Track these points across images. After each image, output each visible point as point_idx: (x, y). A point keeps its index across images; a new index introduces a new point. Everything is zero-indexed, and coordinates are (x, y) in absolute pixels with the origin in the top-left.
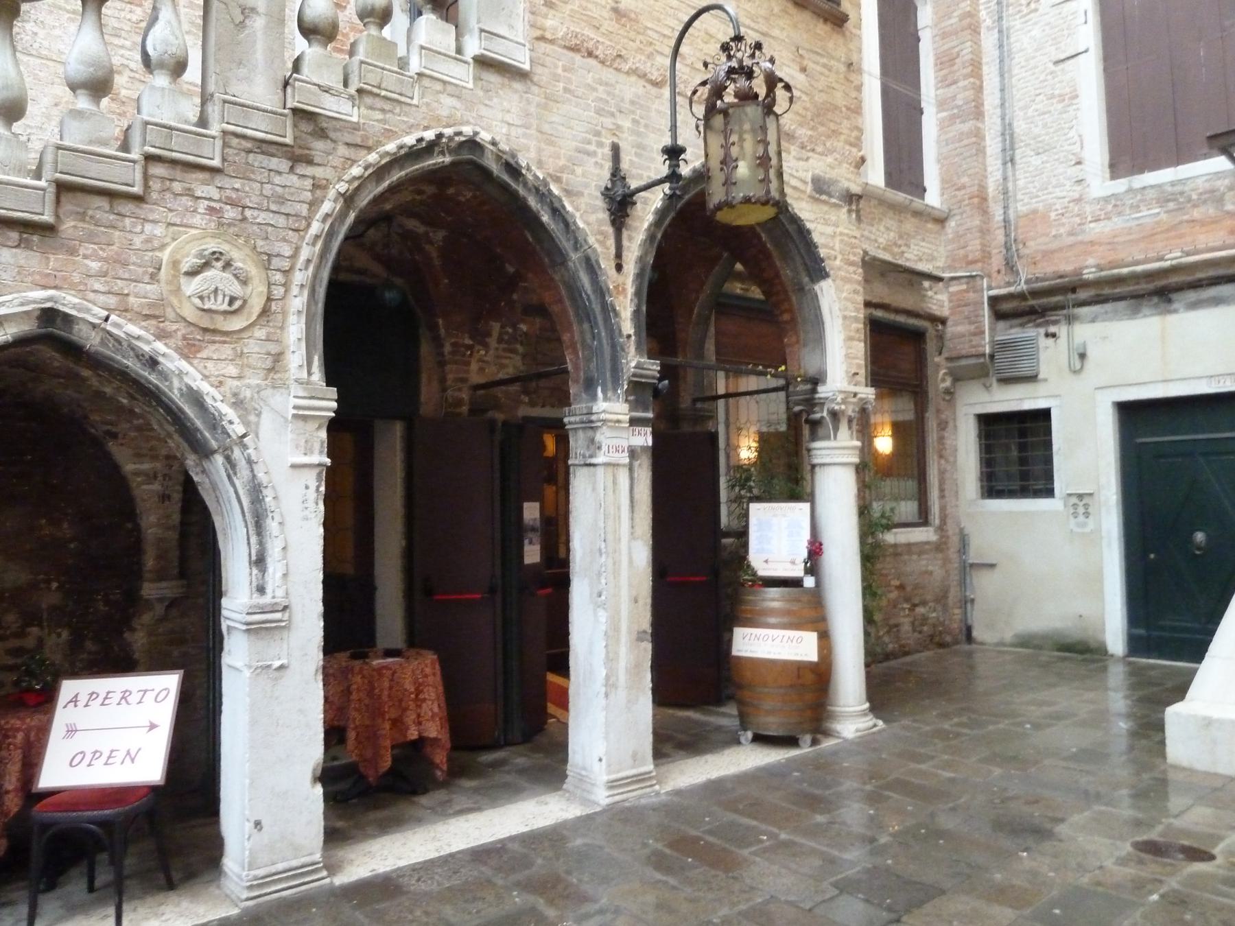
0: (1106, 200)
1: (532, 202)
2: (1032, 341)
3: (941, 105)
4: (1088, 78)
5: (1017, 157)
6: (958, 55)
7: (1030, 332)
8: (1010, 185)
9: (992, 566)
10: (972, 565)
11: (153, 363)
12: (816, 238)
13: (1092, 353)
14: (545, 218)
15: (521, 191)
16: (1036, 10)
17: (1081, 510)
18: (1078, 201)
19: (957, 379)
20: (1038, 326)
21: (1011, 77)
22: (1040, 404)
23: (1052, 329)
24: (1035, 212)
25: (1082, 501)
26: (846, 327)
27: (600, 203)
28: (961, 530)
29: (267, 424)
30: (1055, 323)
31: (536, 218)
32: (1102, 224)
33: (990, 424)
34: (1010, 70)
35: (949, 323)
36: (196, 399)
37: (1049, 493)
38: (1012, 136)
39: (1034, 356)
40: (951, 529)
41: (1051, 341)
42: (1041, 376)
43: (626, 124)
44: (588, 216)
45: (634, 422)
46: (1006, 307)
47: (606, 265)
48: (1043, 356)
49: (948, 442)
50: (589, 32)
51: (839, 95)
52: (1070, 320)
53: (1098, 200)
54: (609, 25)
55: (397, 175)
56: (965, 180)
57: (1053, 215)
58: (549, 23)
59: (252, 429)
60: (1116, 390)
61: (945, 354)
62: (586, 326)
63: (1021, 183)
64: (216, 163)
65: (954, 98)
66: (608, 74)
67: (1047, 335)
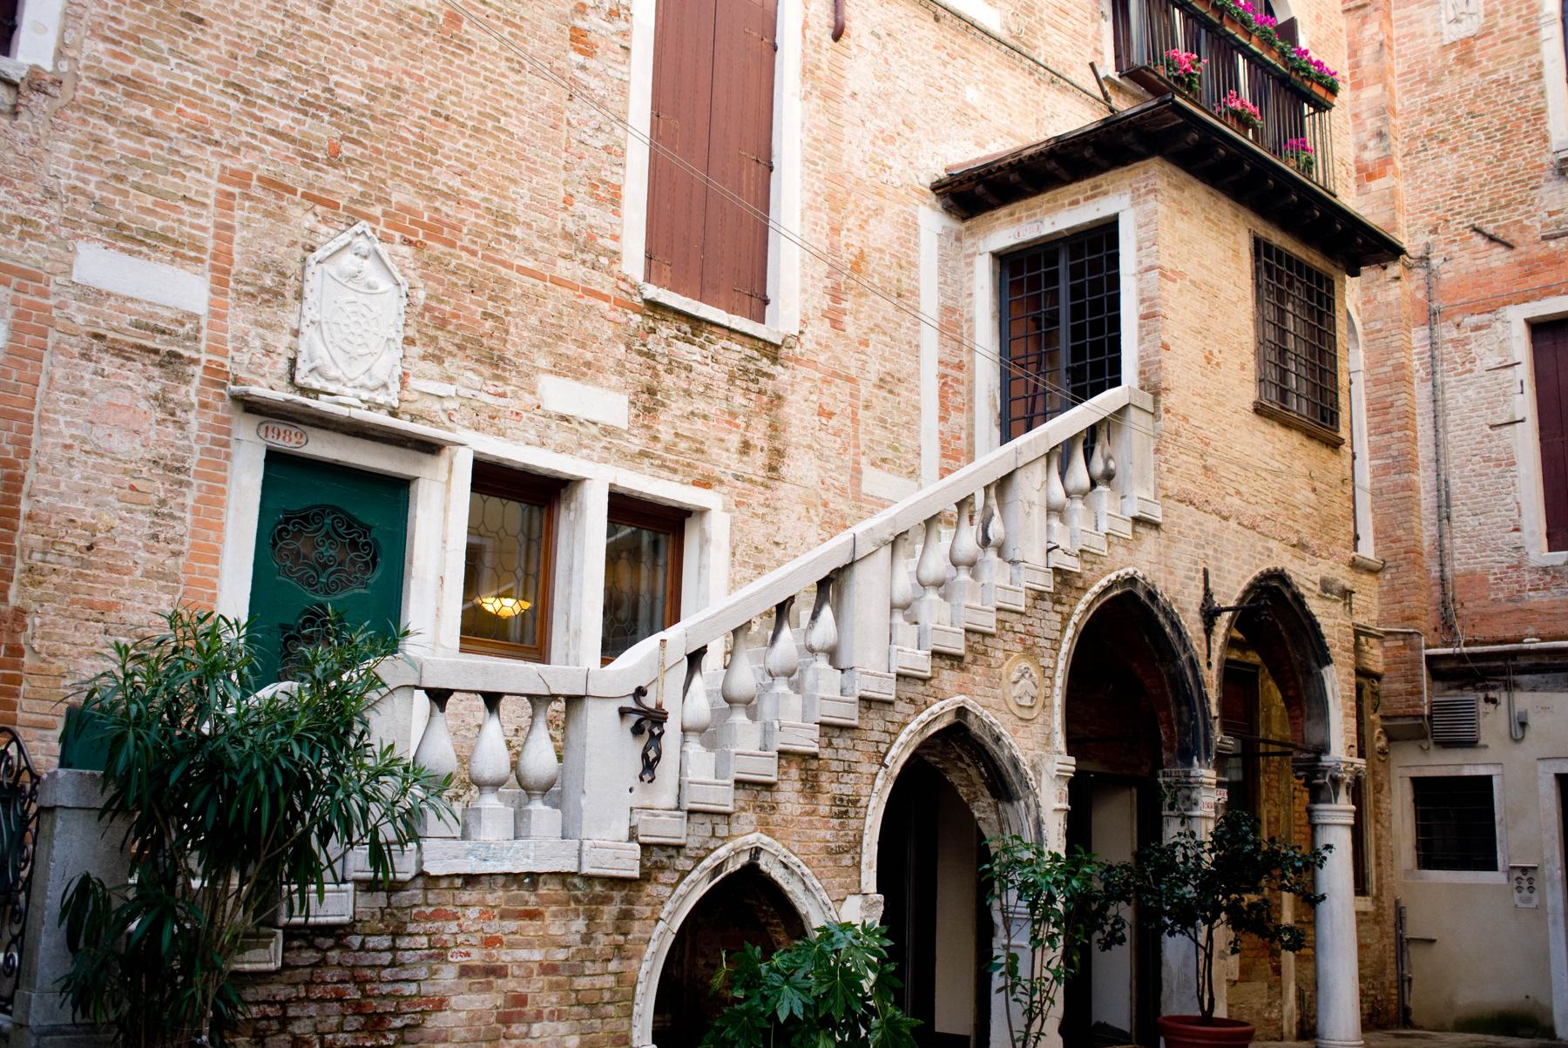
0: (1545, 570)
1: (1161, 618)
2: (1471, 705)
3: (1375, 452)
4: (1526, 444)
5: (1454, 516)
6: (1392, 406)
7: (1469, 695)
8: (1446, 542)
9: (1432, 941)
10: (1408, 940)
11: (998, 739)
12: (1324, 630)
13: (1532, 721)
14: (1168, 630)
16: (1471, 371)
17: (1525, 884)
18: (1517, 567)
19: (1390, 740)
20: (1476, 690)
21: (1446, 433)
22: (1482, 771)
23: (1492, 694)
24: (1472, 573)
25: (1526, 875)
26: (1344, 705)
27: (1198, 617)
28: (1397, 902)
29: (1045, 780)
30: (1494, 688)
31: (1161, 629)
32: (1541, 593)
33: (1424, 789)
34: (1444, 426)
35: (1384, 679)
36: (1015, 762)
37: (1493, 866)
38: (1447, 493)
39: (1472, 720)
40: (1388, 902)
41: (1491, 706)
42: (1481, 742)
43: (1211, 552)
44: (1192, 625)
45: (1219, 784)
46: (1443, 666)
47: (1203, 663)
48: (1484, 722)
49: (1384, 806)
50: (1190, 486)
51: (1337, 506)
52: (1510, 687)
53: (1537, 569)
54: (1201, 479)
55: (1097, 605)
56: (1400, 532)
57: (1491, 578)
58: (1169, 484)
59: (1039, 782)
60: (1557, 762)
61: (1380, 712)
62: (1184, 708)
63: (1458, 542)
64: (1022, 609)
65: (1388, 447)
66: (1199, 515)
67: (1487, 700)
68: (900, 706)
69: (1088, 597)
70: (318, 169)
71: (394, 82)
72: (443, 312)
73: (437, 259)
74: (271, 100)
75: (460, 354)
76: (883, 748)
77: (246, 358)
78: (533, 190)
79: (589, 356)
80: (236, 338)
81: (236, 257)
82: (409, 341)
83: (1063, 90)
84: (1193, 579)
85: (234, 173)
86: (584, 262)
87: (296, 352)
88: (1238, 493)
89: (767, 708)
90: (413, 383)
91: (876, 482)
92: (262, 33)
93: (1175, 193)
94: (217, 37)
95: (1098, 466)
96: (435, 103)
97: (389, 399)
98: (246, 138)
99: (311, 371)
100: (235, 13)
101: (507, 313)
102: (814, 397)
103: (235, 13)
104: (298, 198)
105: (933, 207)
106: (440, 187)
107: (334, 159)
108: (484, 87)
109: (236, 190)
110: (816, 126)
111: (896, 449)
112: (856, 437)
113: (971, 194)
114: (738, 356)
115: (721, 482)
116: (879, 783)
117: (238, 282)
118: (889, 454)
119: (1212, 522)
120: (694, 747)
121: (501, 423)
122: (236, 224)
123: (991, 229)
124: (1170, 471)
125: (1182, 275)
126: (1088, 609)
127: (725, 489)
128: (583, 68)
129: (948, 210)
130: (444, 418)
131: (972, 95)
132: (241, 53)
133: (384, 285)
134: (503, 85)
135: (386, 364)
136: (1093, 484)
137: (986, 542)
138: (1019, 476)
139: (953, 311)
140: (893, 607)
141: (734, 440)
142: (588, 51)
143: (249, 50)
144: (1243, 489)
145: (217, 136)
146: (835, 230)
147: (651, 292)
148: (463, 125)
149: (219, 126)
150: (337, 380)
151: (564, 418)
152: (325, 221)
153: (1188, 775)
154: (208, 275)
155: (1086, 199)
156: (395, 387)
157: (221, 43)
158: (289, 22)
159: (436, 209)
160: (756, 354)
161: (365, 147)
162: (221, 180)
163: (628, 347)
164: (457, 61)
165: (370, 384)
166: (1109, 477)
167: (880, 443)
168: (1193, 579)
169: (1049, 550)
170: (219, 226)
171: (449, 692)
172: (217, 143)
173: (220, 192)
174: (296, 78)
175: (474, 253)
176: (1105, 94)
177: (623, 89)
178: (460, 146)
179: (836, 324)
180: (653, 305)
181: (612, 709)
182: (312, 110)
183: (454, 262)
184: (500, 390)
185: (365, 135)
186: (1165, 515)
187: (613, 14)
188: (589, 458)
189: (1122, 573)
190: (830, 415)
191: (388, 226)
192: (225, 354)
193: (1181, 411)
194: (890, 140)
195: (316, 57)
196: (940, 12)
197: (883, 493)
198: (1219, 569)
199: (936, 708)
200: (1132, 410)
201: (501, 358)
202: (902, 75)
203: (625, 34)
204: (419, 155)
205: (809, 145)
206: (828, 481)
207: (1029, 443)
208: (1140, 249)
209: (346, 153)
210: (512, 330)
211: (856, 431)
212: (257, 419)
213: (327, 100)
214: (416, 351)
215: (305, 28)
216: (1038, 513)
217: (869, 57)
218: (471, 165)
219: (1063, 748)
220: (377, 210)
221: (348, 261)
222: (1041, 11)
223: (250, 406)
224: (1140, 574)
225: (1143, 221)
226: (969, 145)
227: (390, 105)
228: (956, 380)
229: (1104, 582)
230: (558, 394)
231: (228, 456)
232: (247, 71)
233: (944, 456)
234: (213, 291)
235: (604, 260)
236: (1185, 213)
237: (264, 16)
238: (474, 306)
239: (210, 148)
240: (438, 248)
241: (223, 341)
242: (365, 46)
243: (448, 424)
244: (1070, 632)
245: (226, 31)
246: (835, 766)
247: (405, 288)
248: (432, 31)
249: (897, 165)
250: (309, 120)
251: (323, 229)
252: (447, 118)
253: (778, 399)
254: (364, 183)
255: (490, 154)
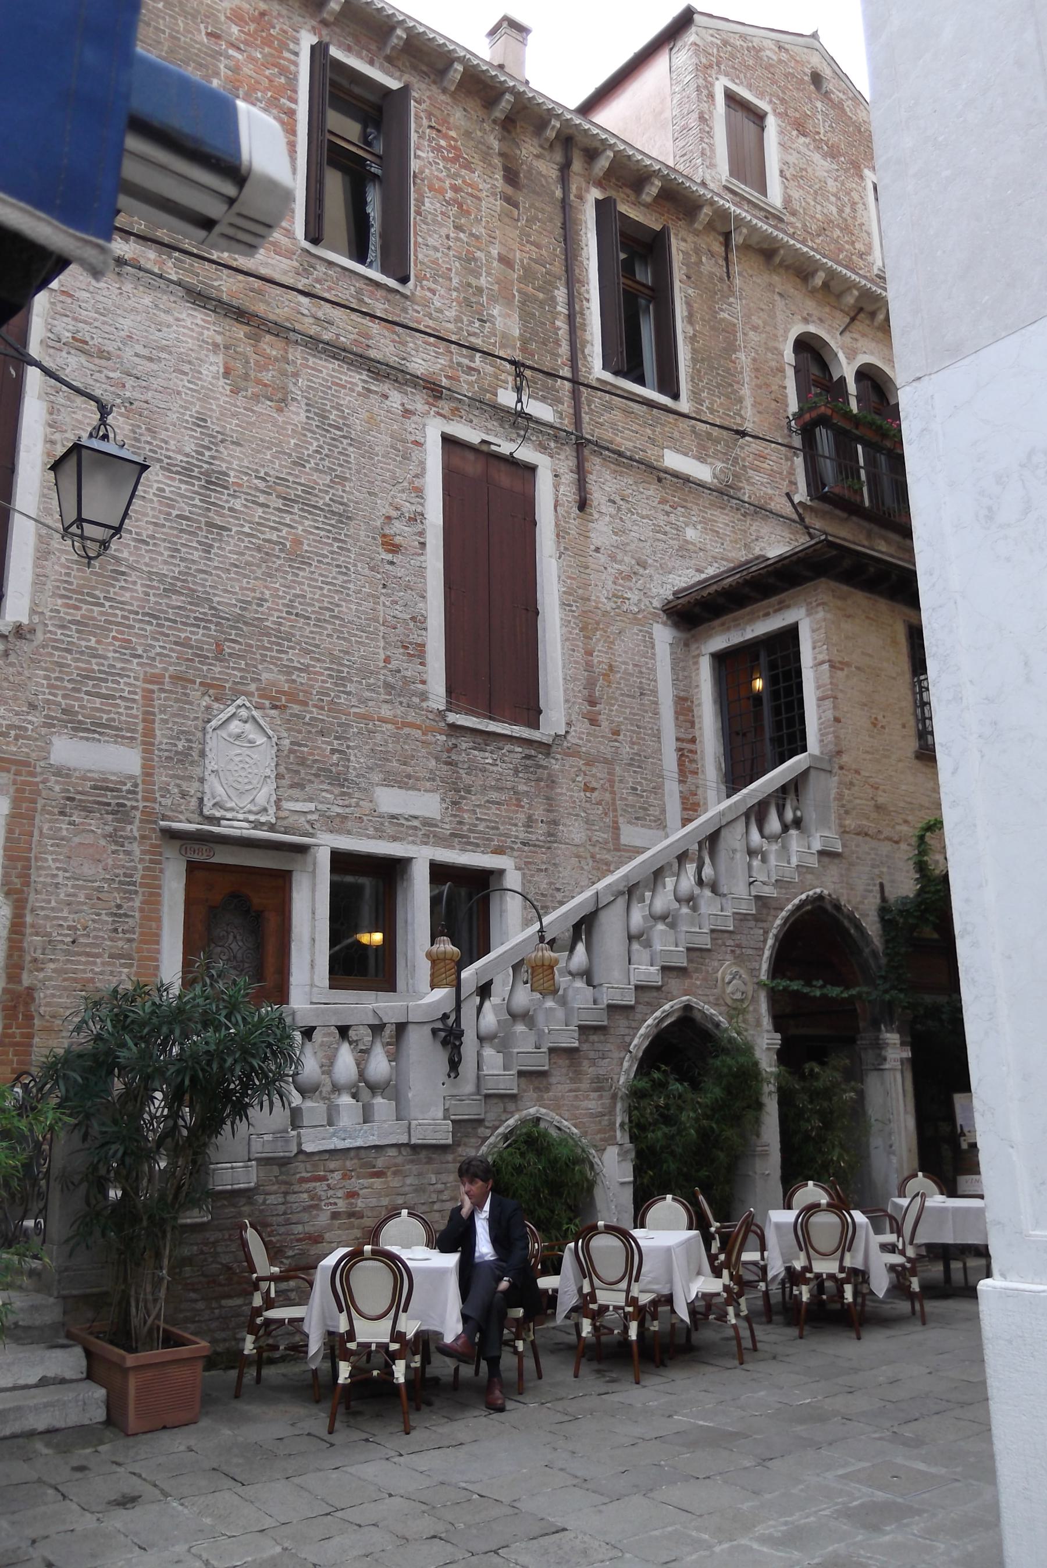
1: (846, 923)
14: (852, 931)
15: (841, 917)
31: (847, 931)
43: (885, 870)
50: (865, 822)
54: (874, 815)
58: (847, 822)
68: (640, 1008)
69: (784, 914)
70: (210, 664)
71: (258, 595)
72: (302, 752)
73: (296, 715)
74: (175, 622)
75: (316, 780)
76: (627, 1039)
77: (169, 802)
78: (362, 657)
79: (409, 769)
80: (161, 788)
81: (158, 733)
82: (279, 776)
83: (765, 518)
84: (871, 891)
85: (154, 675)
86: (401, 703)
87: (203, 793)
88: (906, 821)
89: (540, 1019)
90: (286, 805)
91: (630, 834)
92: (165, 576)
93: (839, 603)
94: (135, 583)
95: (789, 815)
96: (287, 606)
97: (268, 818)
98: (158, 650)
99: (214, 805)
100: (147, 565)
101: (348, 747)
102: (579, 779)
103: (147, 565)
104: (197, 687)
105: (665, 624)
106: (296, 664)
107: (219, 654)
108: (321, 589)
109: (155, 687)
110: (569, 578)
111: (646, 809)
112: (614, 804)
113: (691, 614)
114: (519, 756)
115: (512, 849)
116: (626, 1064)
117: (160, 750)
118: (641, 813)
119: (886, 848)
120: (488, 1052)
121: (349, 824)
122: (156, 710)
123: (710, 636)
124: (847, 812)
125: (848, 664)
126: (785, 923)
127: (516, 854)
128: (392, 563)
129: (676, 625)
130: (308, 827)
131: (691, 534)
132: (152, 592)
133: (261, 740)
134: (334, 585)
135: (265, 794)
136: (785, 828)
137: (700, 882)
138: (723, 833)
139: (685, 699)
140: (631, 938)
141: (521, 817)
142: (392, 547)
143: (158, 588)
144: (910, 818)
145: (140, 652)
146: (589, 653)
147: (452, 718)
148: (309, 618)
149: (141, 644)
150: (232, 809)
151: (393, 817)
152: (216, 700)
153: (878, 1038)
154: (140, 748)
155: (776, 611)
156: (272, 810)
157: (138, 587)
158: (183, 564)
159: (294, 681)
160: (533, 753)
161: (240, 643)
162: (145, 681)
163: (437, 759)
164: (301, 574)
165: (254, 809)
166: (797, 823)
167: (633, 806)
168: (871, 891)
169: (751, 883)
170: (146, 713)
171: (314, 1028)
172: (140, 656)
173: (144, 690)
174: (190, 603)
175: (322, 708)
176: (799, 515)
177: (422, 569)
178: (307, 633)
179: (594, 722)
180: (455, 729)
181: (427, 1030)
182: (203, 624)
183: (308, 716)
184: (346, 803)
185: (240, 636)
186: (844, 846)
187: (412, 520)
188: (414, 842)
189: (811, 893)
190: (593, 790)
191: (260, 697)
192: (154, 800)
193: (854, 766)
194: (628, 578)
195: (204, 586)
196: (662, 475)
197: (638, 843)
198: (893, 881)
199: (667, 1007)
200: (813, 772)
201: (346, 780)
202: (636, 528)
203: (421, 533)
204: (279, 644)
205: (565, 592)
206: (595, 838)
207: (730, 807)
208: (814, 648)
209: (228, 650)
210: (352, 758)
211: (614, 799)
212: (178, 843)
213: (213, 615)
214: (286, 782)
215: (194, 567)
216: (741, 857)
217: (607, 518)
218: (317, 646)
219: (770, 1027)
220: (253, 687)
221: (235, 726)
222: (744, 460)
223: (172, 835)
224: (826, 892)
225: (815, 627)
226: (691, 572)
227: (257, 612)
228: (691, 751)
229: (796, 901)
230: (391, 800)
231: (161, 871)
232: (156, 603)
233: (684, 809)
234: (143, 758)
235: (416, 700)
236: (849, 616)
237: (166, 562)
238: (324, 745)
239: (135, 661)
240: (296, 708)
241: (153, 792)
242: (236, 573)
243: (311, 831)
244: (770, 942)
245: (142, 578)
246: (592, 1054)
247: (275, 740)
248: (283, 555)
249: (634, 596)
250: (201, 631)
251: (216, 705)
252: (297, 615)
253: (552, 783)
254: (240, 670)
255: (329, 636)
